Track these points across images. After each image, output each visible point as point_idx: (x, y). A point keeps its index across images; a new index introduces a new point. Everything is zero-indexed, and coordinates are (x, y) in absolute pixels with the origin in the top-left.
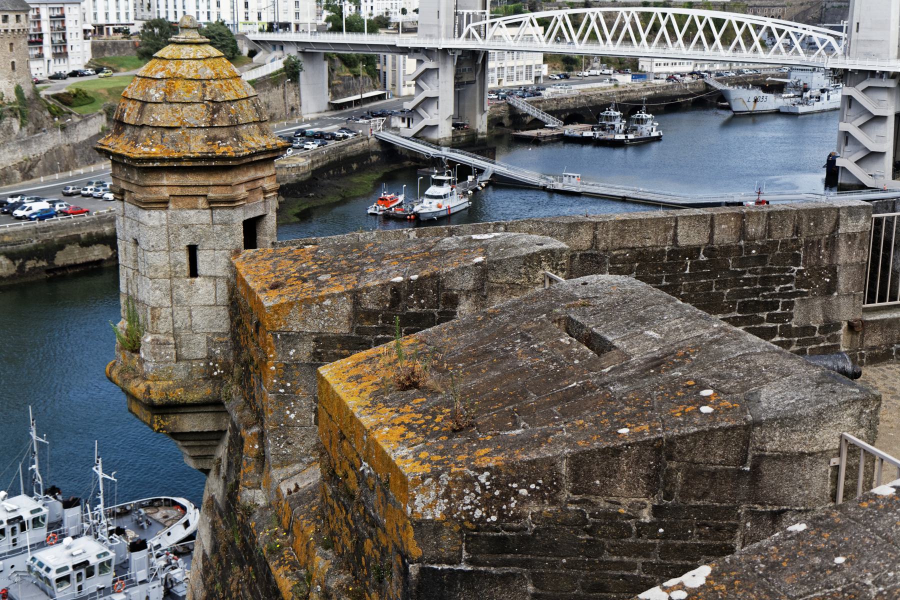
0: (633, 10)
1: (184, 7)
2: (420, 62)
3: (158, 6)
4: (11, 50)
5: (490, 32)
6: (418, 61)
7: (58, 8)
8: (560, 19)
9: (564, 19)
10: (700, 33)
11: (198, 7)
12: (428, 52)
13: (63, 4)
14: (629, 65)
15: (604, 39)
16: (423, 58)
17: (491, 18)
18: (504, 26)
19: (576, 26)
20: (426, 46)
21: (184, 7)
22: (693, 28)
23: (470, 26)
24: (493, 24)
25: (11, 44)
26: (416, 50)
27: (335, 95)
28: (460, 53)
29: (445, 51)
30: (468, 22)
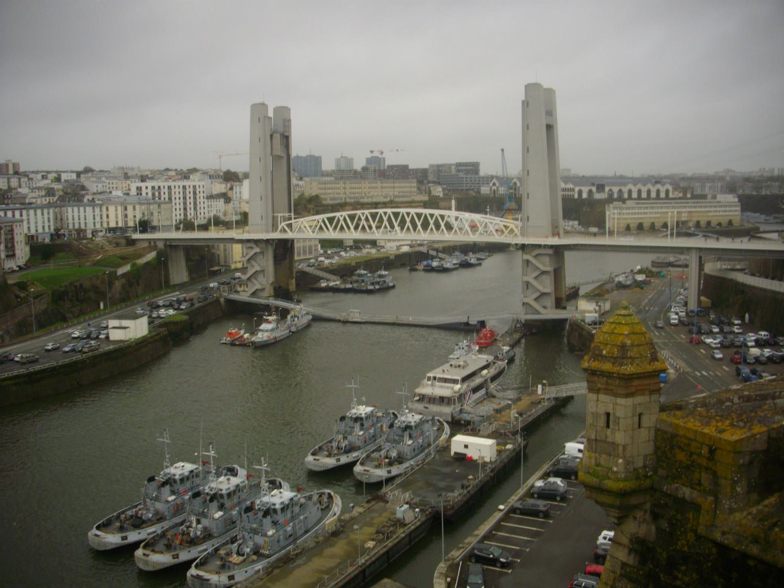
1: (85, 219)
3: (67, 219)
7: (9, 226)
8: (341, 219)
11: (94, 219)
12: (257, 242)
13: (13, 222)
16: (253, 245)
17: (295, 218)
21: (85, 219)
23: (283, 224)
26: (248, 241)
28: (277, 241)
29: (267, 241)
30: (281, 223)
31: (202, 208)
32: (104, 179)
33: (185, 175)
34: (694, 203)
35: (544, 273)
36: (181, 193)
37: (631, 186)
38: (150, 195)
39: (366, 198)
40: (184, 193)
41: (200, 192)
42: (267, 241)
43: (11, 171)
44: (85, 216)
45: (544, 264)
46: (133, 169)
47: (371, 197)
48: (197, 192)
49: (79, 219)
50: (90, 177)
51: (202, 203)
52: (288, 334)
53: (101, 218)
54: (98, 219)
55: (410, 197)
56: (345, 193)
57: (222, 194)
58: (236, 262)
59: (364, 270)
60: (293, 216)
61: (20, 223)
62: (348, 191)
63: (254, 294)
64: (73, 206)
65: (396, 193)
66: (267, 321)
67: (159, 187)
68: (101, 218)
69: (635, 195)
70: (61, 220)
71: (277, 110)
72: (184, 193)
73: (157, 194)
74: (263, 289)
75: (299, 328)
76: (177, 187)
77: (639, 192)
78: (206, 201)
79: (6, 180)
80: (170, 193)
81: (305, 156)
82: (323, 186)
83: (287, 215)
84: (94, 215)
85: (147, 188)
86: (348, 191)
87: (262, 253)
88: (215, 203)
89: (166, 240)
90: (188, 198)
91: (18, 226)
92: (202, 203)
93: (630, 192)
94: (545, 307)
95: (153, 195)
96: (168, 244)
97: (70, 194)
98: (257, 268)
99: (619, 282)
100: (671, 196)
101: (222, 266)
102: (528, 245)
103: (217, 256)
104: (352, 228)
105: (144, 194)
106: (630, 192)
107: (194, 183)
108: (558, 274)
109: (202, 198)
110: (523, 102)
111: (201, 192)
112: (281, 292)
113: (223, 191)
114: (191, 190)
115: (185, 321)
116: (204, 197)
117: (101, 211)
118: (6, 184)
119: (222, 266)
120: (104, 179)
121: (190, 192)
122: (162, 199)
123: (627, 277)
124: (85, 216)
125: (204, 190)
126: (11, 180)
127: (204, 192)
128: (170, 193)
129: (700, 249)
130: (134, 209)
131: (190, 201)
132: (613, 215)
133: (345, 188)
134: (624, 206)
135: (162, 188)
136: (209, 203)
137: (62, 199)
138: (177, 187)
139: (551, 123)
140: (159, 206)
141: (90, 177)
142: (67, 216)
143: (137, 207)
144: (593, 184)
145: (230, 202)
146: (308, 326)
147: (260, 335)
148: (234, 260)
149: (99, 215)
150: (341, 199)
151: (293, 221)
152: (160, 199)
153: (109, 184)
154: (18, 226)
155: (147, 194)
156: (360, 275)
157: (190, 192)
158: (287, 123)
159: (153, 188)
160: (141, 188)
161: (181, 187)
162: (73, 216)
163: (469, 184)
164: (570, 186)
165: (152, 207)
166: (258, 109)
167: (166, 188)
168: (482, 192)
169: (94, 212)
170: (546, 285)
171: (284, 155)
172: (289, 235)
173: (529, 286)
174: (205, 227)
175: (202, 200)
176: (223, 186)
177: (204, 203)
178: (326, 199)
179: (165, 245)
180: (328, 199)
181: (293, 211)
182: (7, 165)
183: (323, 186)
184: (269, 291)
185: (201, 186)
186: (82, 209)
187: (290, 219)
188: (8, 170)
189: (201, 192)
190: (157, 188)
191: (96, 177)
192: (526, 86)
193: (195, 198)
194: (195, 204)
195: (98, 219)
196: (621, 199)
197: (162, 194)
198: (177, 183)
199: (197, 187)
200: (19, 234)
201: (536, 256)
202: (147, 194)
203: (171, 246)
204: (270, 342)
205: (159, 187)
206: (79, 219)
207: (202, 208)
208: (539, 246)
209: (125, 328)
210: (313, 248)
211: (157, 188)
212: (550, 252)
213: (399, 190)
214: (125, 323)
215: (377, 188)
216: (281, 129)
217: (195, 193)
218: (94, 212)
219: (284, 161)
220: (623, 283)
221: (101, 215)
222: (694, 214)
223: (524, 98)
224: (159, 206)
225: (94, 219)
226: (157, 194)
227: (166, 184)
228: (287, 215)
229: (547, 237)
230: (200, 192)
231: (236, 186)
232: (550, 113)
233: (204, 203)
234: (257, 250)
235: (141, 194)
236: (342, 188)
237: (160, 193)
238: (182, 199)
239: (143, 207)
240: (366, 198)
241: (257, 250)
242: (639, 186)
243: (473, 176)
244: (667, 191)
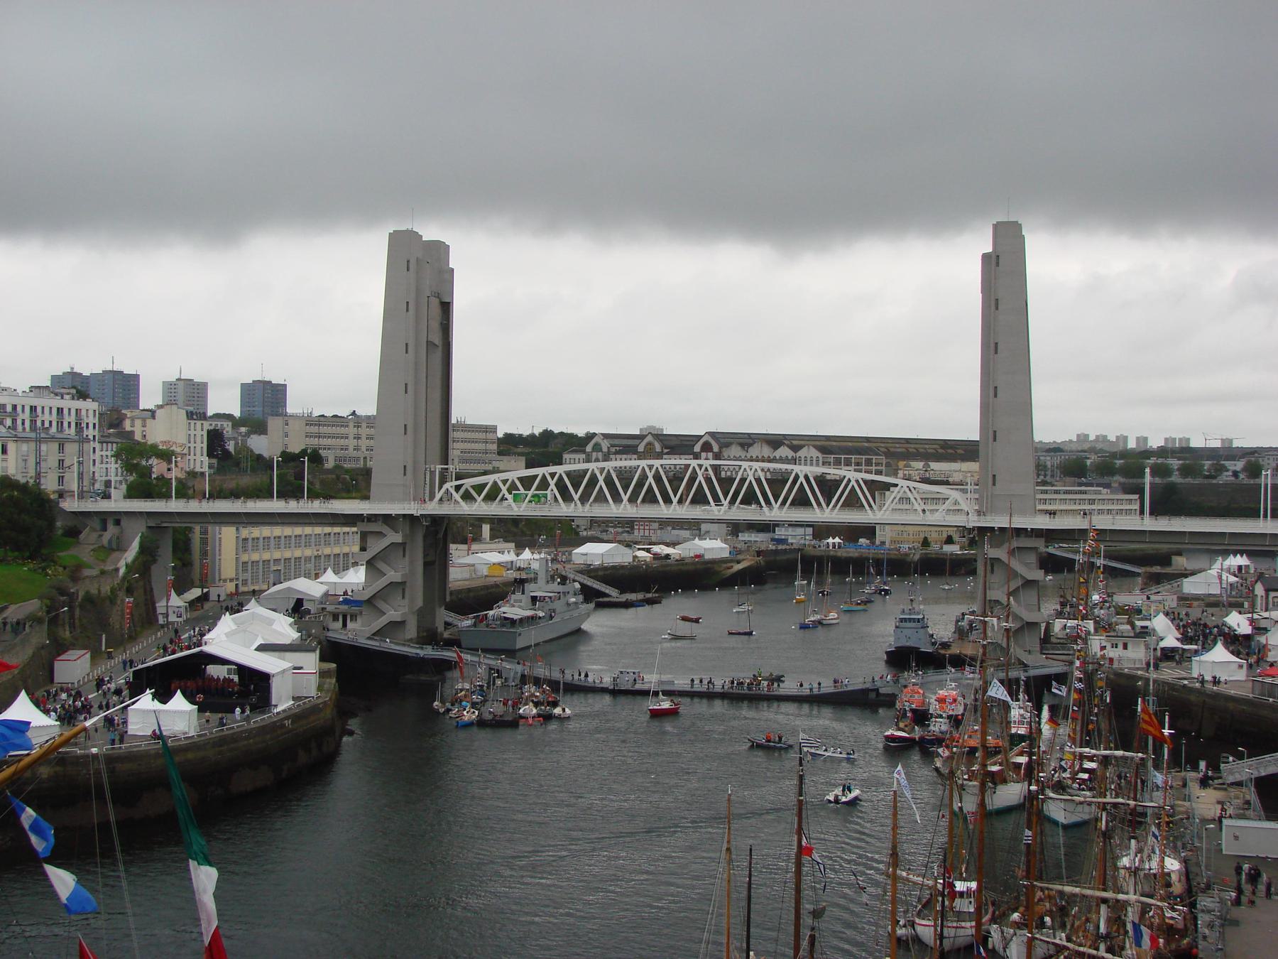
16: (385, 529)
23: (446, 486)
26: (372, 518)
42: (410, 518)
48: (84, 425)
58: (225, 581)
63: (379, 633)
67: (15, 407)
76: (47, 410)
82: (314, 429)
87: (403, 545)
98: (393, 575)
114: (73, 419)
133: (358, 437)
135: (19, 409)
138: (47, 410)
140: (61, 448)
148: (223, 577)
161: (54, 411)
165: (44, 447)
167: (27, 409)
171: (437, 339)
183: (314, 429)
184: (411, 631)
205: (15, 407)
211: (9, 409)
219: (438, 355)
231: (133, 419)
234: (397, 538)
239: (24, 447)
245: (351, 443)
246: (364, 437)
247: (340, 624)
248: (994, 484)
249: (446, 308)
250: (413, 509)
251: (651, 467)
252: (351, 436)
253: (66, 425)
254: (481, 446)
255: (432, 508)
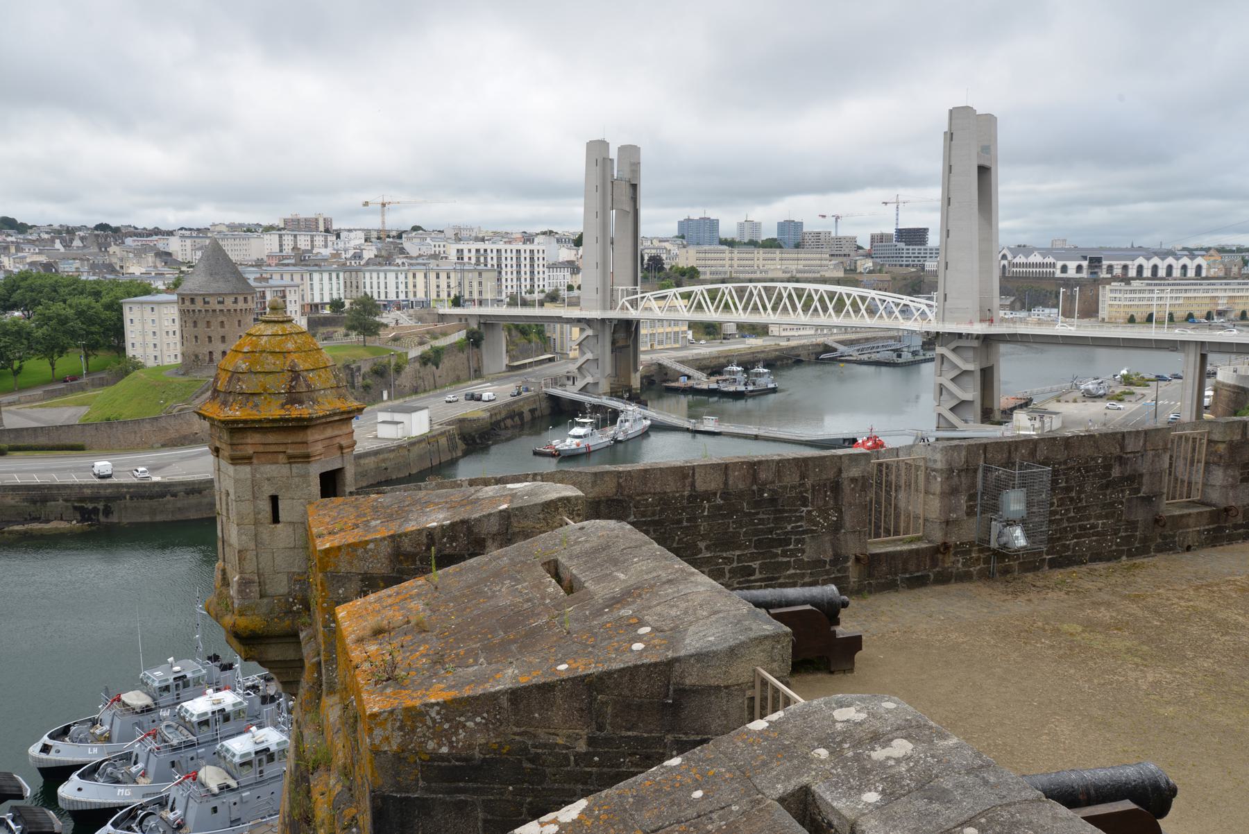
0: (760, 285)
1: (386, 288)
2: (582, 330)
4: (239, 325)
5: (642, 305)
6: (581, 329)
9: (702, 294)
10: (816, 303)
11: (397, 288)
12: (589, 322)
13: (285, 287)
14: (760, 330)
15: (736, 308)
16: (586, 326)
17: (642, 293)
18: (652, 299)
19: (713, 299)
20: (587, 317)
21: (386, 288)
22: (780, 297)
23: (624, 300)
24: (643, 298)
25: (239, 321)
26: (579, 320)
27: (512, 358)
29: (603, 320)
31: (541, 279)
32: (428, 240)
33: (528, 238)
34: (1239, 284)
35: (965, 373)
36: (514, 259)
37: (1141, 260)
38: (473, 261)
39: (758, 272)
40: (518, 259)
41: (538, 258)
43: (322, 228)
44: (386, 283)
45: (966, 360)
46: (471, 229)
47: (766, 272)
48: (536, 259)
49: (379, 288)
50: (412, 238)
51: (541, 273)
52: (608, 443)
53: (406, 287)
54: (402, 287)
55: (819, 272)
56: (731, 266)
57: (568, 262)
59: (764, 367)
60: (639, 290)
61: (296, 289)
62: (736, 263)
63: (584, 390)
64: (371, 271)
65: (801, 267)
66: (583, 425)
67: (485, 250)
68: (406, 287)
69: (1147, 273)
70: (357, 287)
71: (622, 149)
72: (518, 259)
73: (482, 259)
74: (596, 384)
75: (629, 437)
76: (509, 251)
77: (1155, 268)
78: (546, 270)
79: (309, 238)
80: (499, 259)
81: (697, 218)
83: (630, 288)
84: (397, 283)
85: (470, 251)
86: (736, 263)
88: (562, 274)
89: (480, 316)
90: (522, 266)
91: (293, 292)
92: (541, 273)
93: (1140, 269)
94: (966, 421)
95: (478, 259)
96: (482, 321)
97: (382, 257)
99: (1087, 391)
100: (1204, 274)
101: (557, 353)
102: (944, 334)
103: (552, 340)
104: (740, 308)
105: (466, 260)
106: (1140, 269)
107: (538, 247)
108: (987, 377)
109: (541, 266)
110: (945, 133)
111: (541, 259)
112: (621, 391)
113: (573, 258)
115: (483, 419)
116: (544, 265)
117: (406, 278)
118: (309, 243)
119: (557, 353)
120: (428, 240)
121: (525, 258)
122: (489, 266)
123: (1099, 384)
124: (386, 283)
125: (545, 256)
126: (298, 238)
127: (544, 259)
128: (499, 259)
129: (1203, 343)
130: (448, 277)
131: (526, 269)
132: (1111, 299)
133: (731, 259)
134: (1127, 288)
135: (489, 251)
136: (551, 274)
137: (367, 264)
138: (509, 251)
139: (986, 164)
140: (480, 274)
141: (412, 238)
142: (364, 283)
143: (452, 275)
144: (1085, 258)
145: (578, 273)
146: (645, 434)
147: (569, 441)
149: (404, 283)
150: (725, 273)
151: (639, 296)
152: (486, 265)
153: (435, 246)
154: (293, 292)
155: (470, 258)
156: (733, 373)
157: (525, 258)
158: (635, 167)
159: (478, 251)
160: (462, 250)
161: (514, 252)
162: (371, 283)
163: (910, 257)
164: (1051, 260)
166: (597, 151)
167: (495, 251)
168: (927, 268)
169: (397, 278)
170: (971, 393)
172: (632, 314)
173: (944, 392)
174: (541, 304)
175: (541, 269)
176: (574, 252)
177: (544, 272)
178: (705, 273)
179: (479, 324)
180: (708, 274)
181: (639, 283)
182: (317, 220)
184: (605, 386)
185: (541, 252)
186: (382, 275)
187: (637, 293)
188: (317, 227)
189: (541, 259)
190: (482, 251)
191: (421, 238)
192: (951, 111)
193: (532, 266)
194: (532, 273)
195: (402, 287)
196: (1126, 279)
197: (489, 259)
198: (509, 247)
199: (536, 252)
200: (293, 302)
201: (954, 350)
202: (470, 258)
203: (488, 323)
204: (580, 451)
205: (485, 250)
206: (379, 288)
207: (541, 279)
208: (960, 335)
209: (397, 423)
210: (681, 336)
211: (482, 251)
212: (975, 344)
213: (807, 262)
214: (398, 417)
215: (774, 259)
216: (627, 175)
217: (532, 259)
218: (397, 278)
219: (630, 218)
220: (1094, 392)
221: (406, 283)
222: (1237, 301)
223: (946, 129)
224: (480, 274)
225: (397, 288)
226: (482, 259)
227: (495, 247)
228: (630, 288)
229: (971, 323)
230: (538, 258)
232: (988, 148)
233: (544, 272)
235: (462, 259)
236: (736, 259)
237: (486, 259)
238: (515, 266)
240: (758, 272)
241: (589, 332)
242: (1155, 260)
243: (917, 247)
244: (1199, 268)
245: (727, 263)
246: (736, 259)
247: (571, 382)
248: (945, 300)
249: (634, 187)
250: (597, 314)
251: (727, 288)
252: (727, 259)
253: (522, 259)
254: (818, 262)
255: (616, 314)
